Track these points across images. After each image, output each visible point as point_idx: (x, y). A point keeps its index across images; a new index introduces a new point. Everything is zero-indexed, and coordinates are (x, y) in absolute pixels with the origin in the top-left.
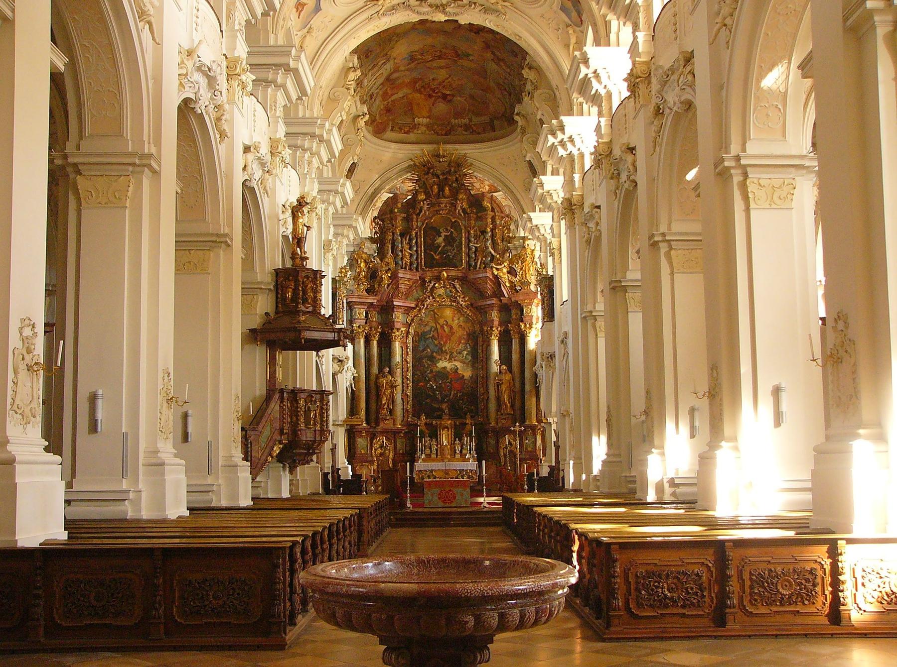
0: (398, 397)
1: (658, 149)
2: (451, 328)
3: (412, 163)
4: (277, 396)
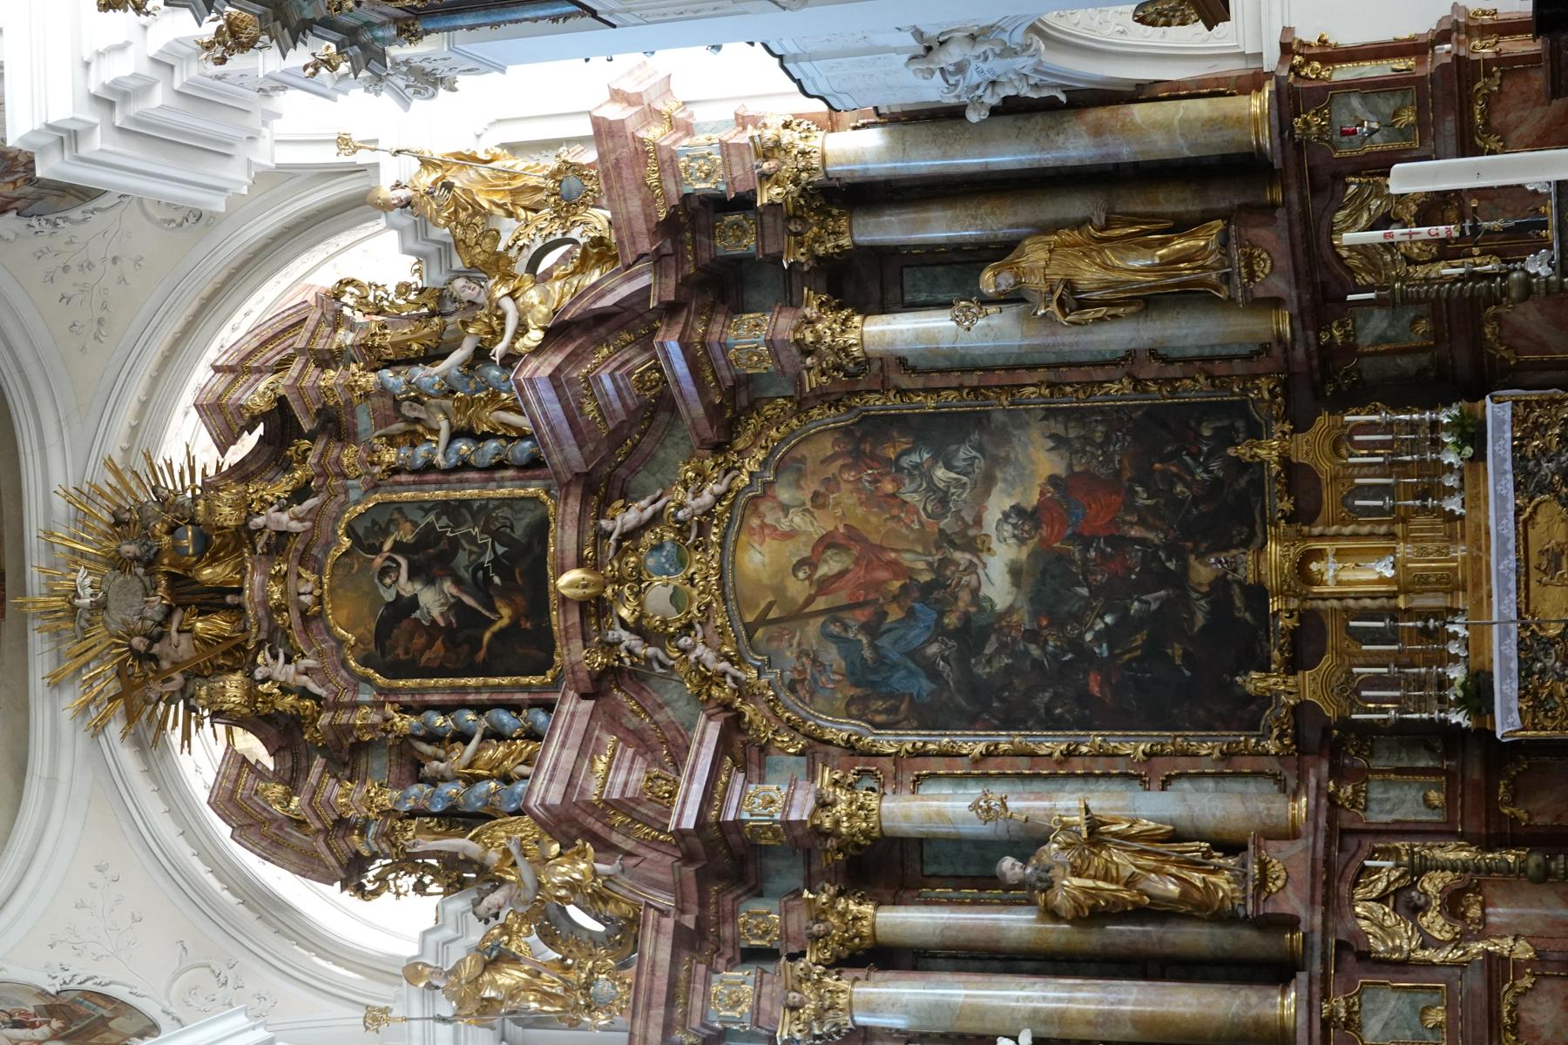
0: (1151, 807)
2: (827, 543)
3: (115, 728)
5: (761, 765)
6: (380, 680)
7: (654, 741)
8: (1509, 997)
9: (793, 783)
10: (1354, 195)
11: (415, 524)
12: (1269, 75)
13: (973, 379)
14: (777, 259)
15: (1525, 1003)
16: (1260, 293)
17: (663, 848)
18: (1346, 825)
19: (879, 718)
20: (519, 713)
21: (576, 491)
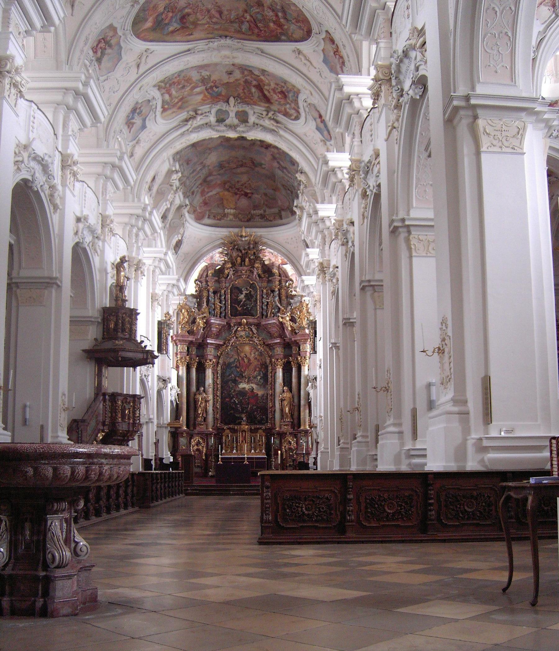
0: (210, 409)
1: (365, 221)
2: (249, 360)
3: (223, 241)
4: (101, 398)
13: (273, 383)
16: (282, 426)
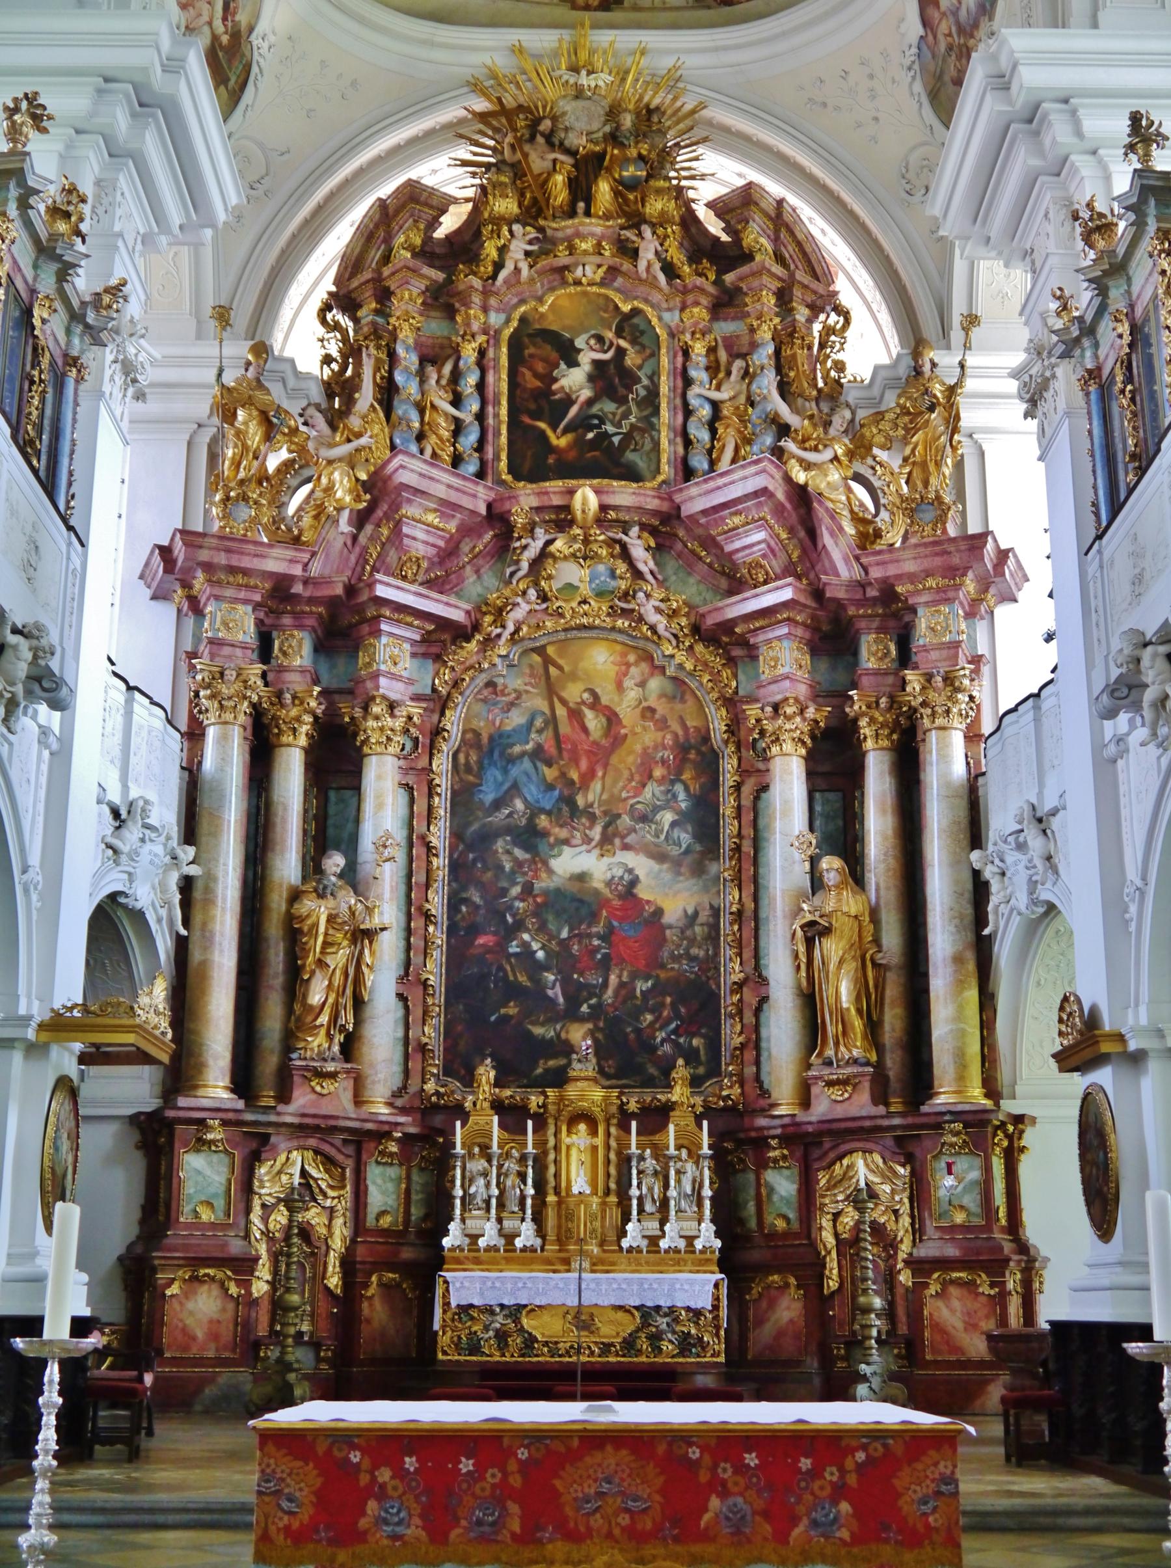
0: (383, 984)
2: (612, 718)
5: (425, 655)
6: (507, 332)
7: (448, 565)
8: (220, 1275)
9: (410, 682)
10: (895, 1172)
11: (640, 368)
12: (997, 1104)
13: (747, 847)
14: (854, 686)
15: (215, 1290)
16: (815, 1090)
17: (359, 569)
18: (365, 1146)
19: (462, 758)
20: (476, 450)
21: (665, 507)
